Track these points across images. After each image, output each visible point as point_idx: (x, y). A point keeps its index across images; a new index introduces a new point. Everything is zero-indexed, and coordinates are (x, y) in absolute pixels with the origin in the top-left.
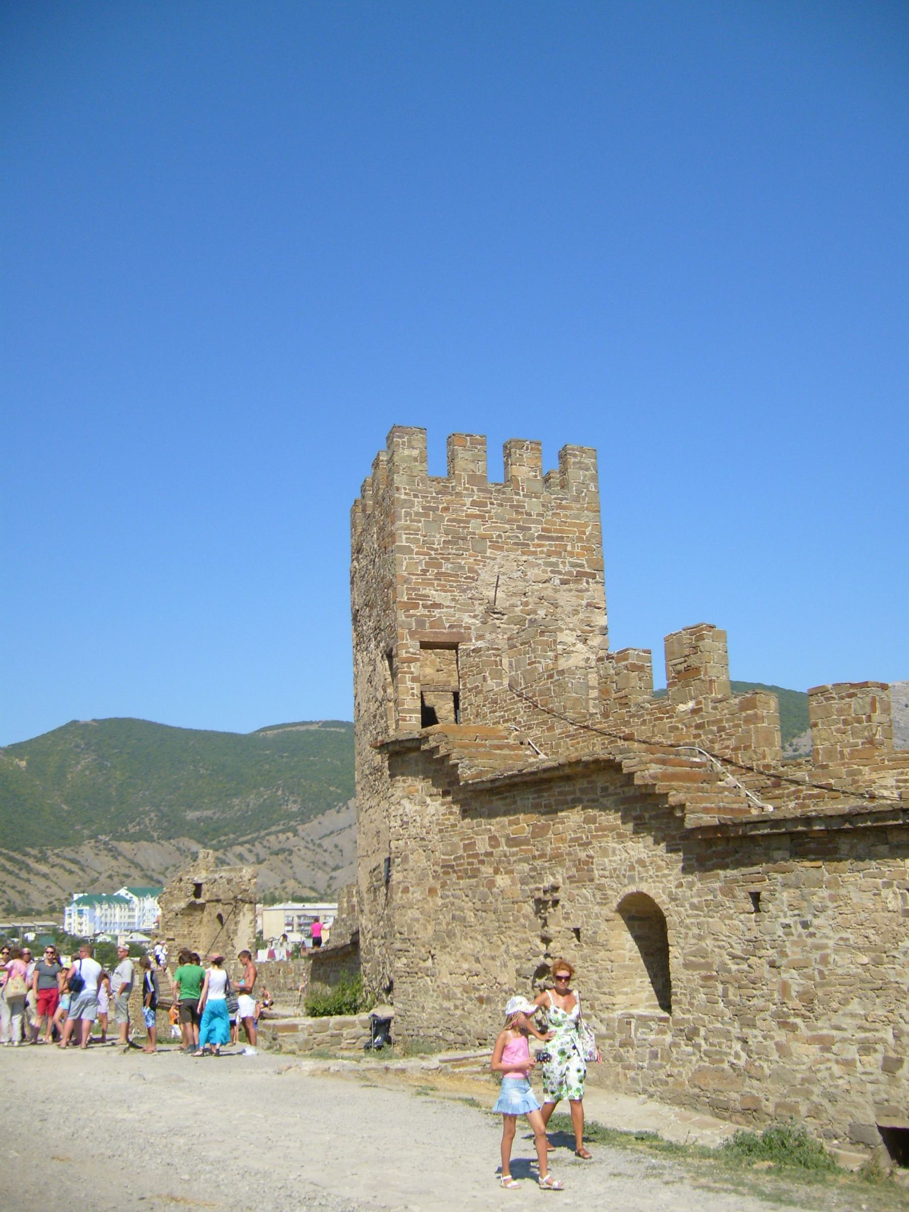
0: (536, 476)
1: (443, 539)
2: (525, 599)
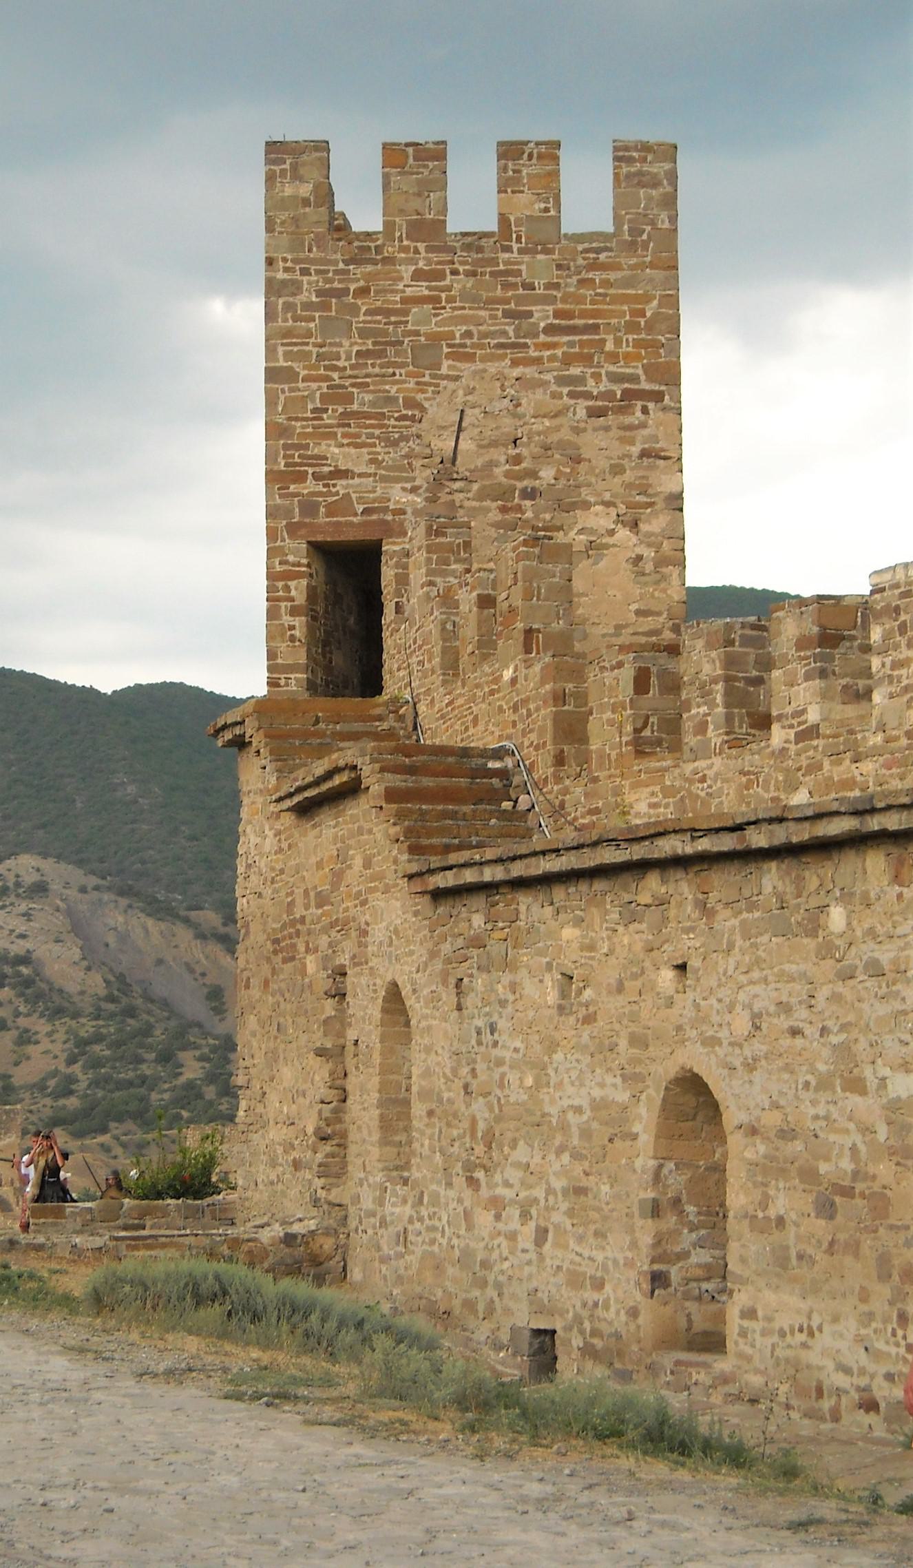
0: (547, 210)
1: (356, 348)
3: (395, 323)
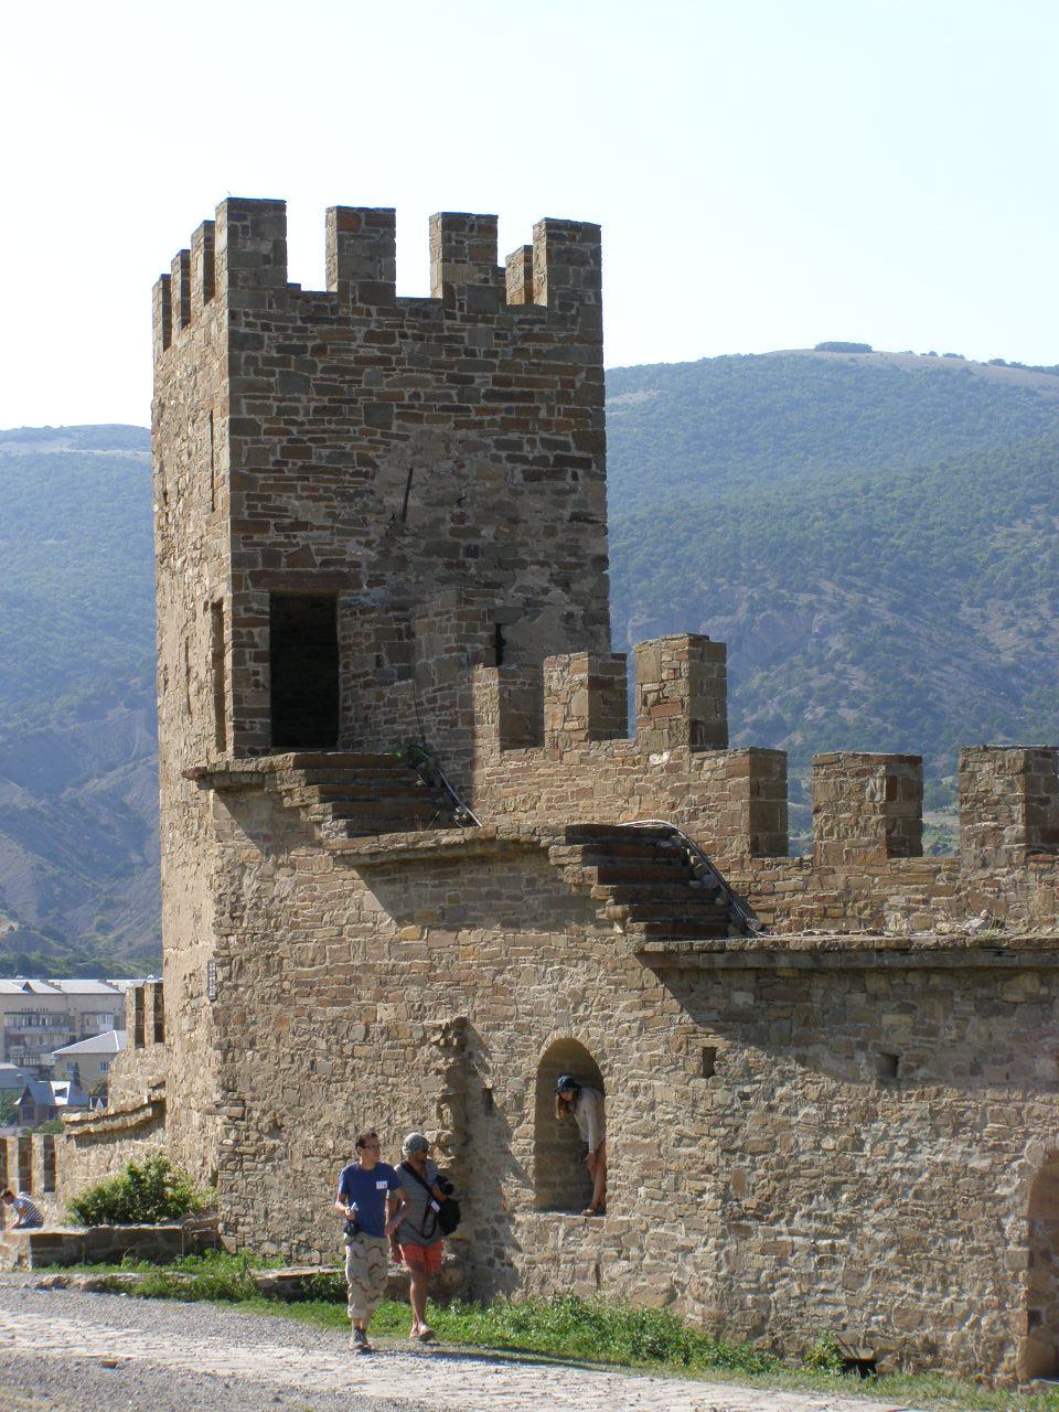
0: (486, 280)
1: (313, 404)
3: (351, 381)
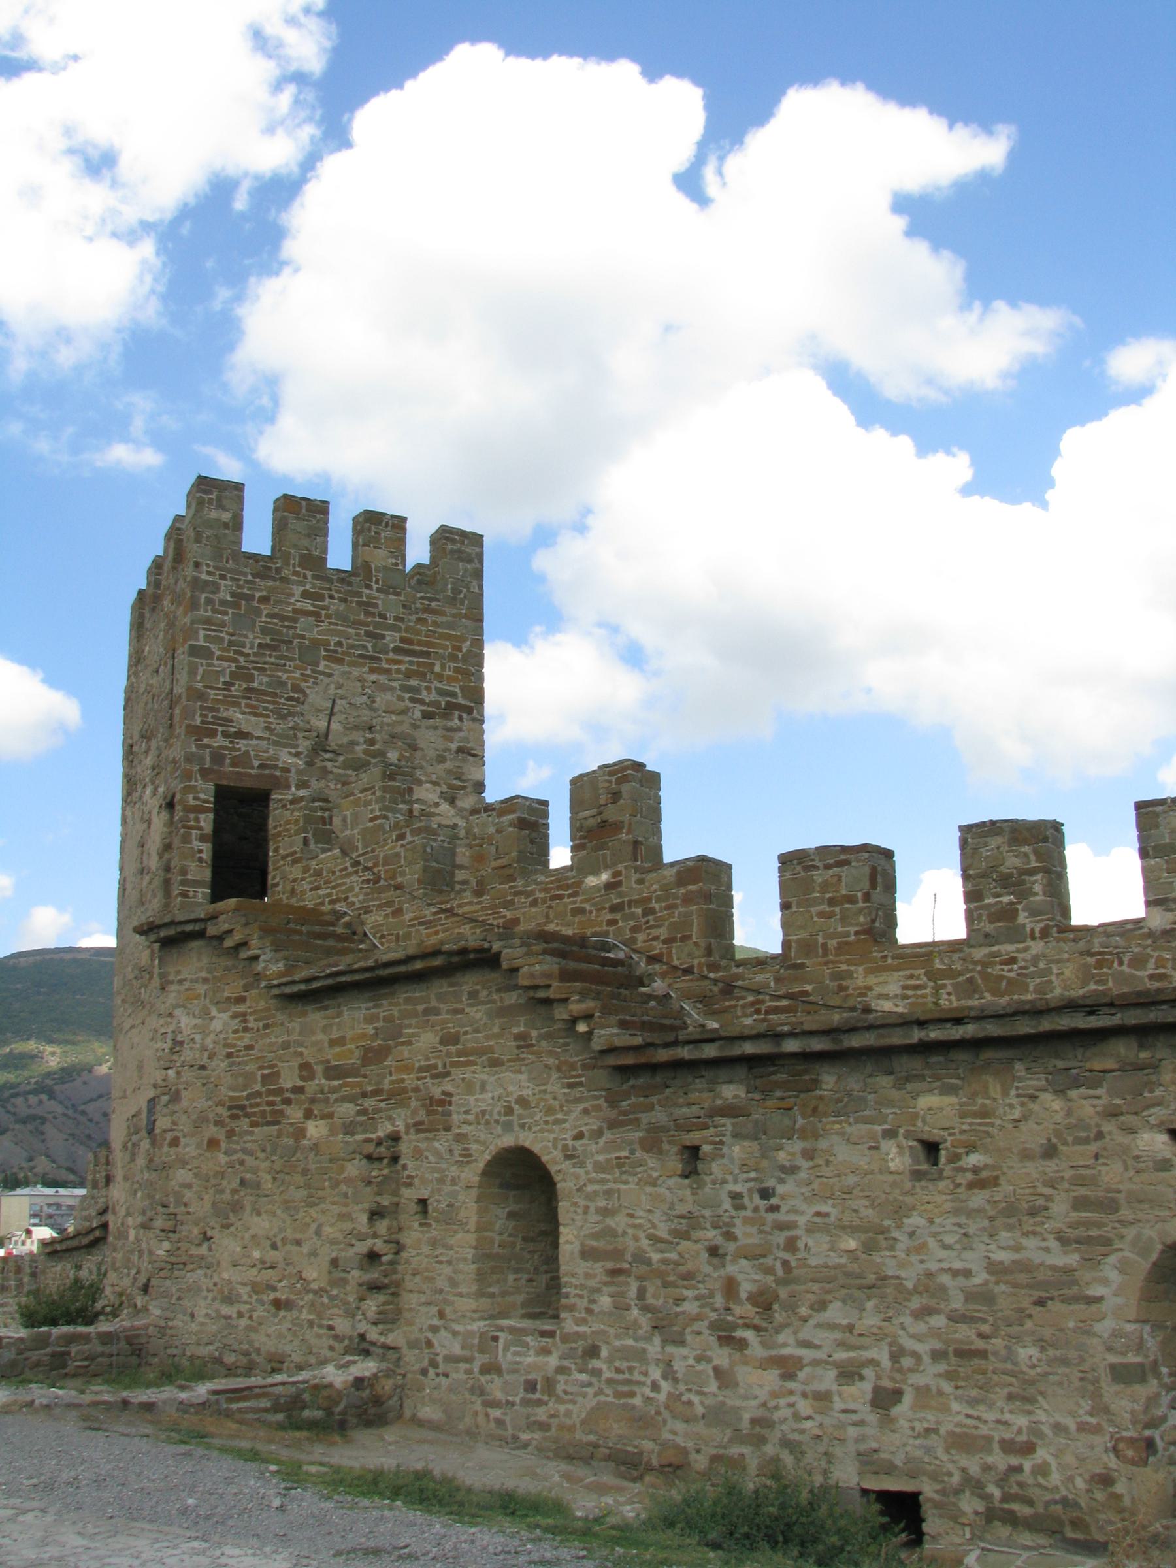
0: (396, 564)
1: (258, 641)
2: (370, 736)
